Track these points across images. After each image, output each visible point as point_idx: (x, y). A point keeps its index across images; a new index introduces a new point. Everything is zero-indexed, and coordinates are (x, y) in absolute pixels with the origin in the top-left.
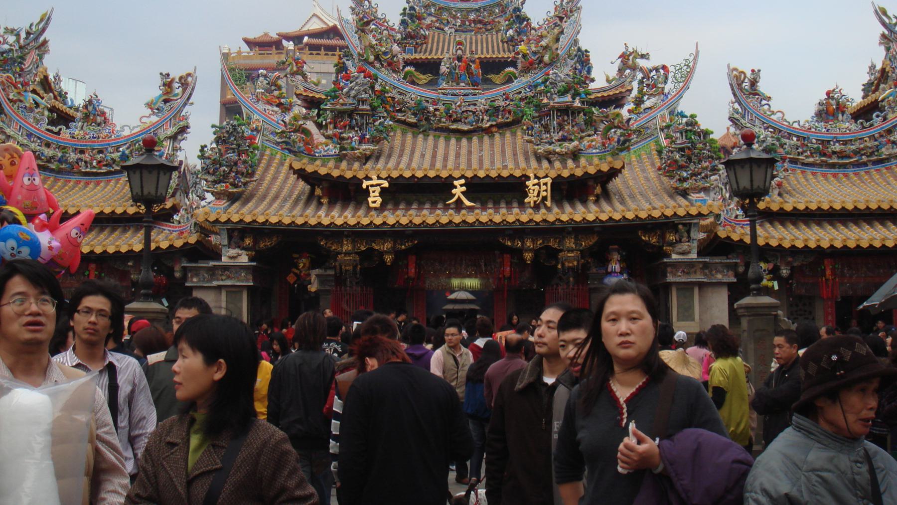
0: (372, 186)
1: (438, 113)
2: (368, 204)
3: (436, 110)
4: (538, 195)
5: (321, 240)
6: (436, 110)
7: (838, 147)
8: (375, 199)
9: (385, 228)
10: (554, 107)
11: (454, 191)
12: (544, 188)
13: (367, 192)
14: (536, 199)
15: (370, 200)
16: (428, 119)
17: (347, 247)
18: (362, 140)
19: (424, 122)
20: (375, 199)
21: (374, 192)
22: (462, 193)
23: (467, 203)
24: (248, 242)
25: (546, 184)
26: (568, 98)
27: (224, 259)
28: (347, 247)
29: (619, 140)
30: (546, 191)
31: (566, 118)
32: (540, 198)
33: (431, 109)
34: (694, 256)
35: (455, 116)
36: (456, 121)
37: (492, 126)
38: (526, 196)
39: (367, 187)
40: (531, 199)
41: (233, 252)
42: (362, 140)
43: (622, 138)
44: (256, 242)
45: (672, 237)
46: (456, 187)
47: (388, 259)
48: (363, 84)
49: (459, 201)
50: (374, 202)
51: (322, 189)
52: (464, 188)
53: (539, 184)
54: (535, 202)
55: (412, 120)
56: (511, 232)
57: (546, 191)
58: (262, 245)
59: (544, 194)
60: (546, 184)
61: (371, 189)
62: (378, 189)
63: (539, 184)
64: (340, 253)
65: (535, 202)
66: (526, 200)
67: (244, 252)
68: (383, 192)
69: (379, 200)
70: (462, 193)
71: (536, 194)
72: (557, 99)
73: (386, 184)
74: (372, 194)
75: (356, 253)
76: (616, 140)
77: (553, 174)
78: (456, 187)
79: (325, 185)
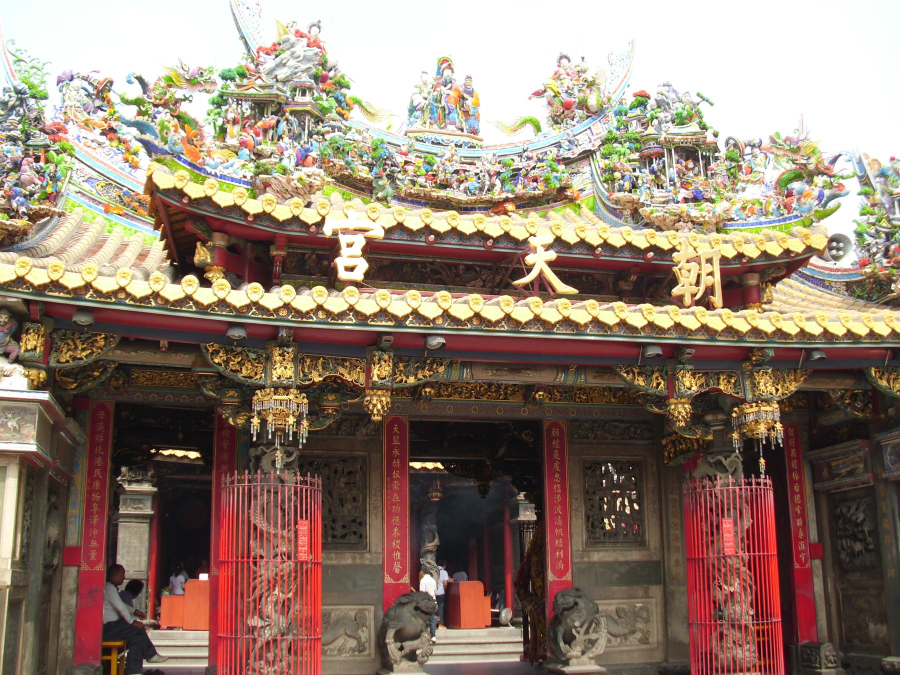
0: (346, 231)
1: (410, 168)
2: (334, 271)
3: (406, 163)
4: (698, 283)
5: (216, 353)
6: (406, 163)
8: (351, 262)
9: (382, 326)
10: (668, 141)
11: (529, 259)
12: (706, 268)
13: (332, 247)
14: (694, 289)
15: (341, 263)
16: (391, 177)
17: (283, 369)
18: (302, 160)
19: (384, 181)
20: (351, 262)
21: (350, 245)
22: (550, 264)
23: (561, 287)
24: (32, 342)
25: (709, 261)
26: (694, 127)
28: (283, 369)
29: (820, 197)
30: (711, 274)
31: (691, 164)
32: (702, 289)
33: (400, 159)
35: (441, 176)
36: (444, 186)
37: (507, 200)
38: (675, 282)
39: (335, 233)
40: (684, 288)
42: (302, 160)
43: (827, 192)
44: (50, 347)
46: (535, 250)
47: (378, 404)
48: (307, 59)
50: (351, 269)
51: (212, 249)
52: (552, 255)
53: (697, 260)
54: (693, 295)
55: (363, 173)
56: (659, 351)
57: (711, 274)
58: (65, 357)
59: (706, 281)
60: (709, 261)
61: (343, 240)
62: (360, 241)
63: (697, 260)
64: (262, 387)
65: (693, 295)
66: (676, 291)
67: (19, 368)
68: (371, 249)
69: (363, 266)
70: (550, 264)
72: (673, 129)
73: (378, 233)
74: (344, 251)
75: (301, 389)
76: (816, 193)
78: (535, 250)
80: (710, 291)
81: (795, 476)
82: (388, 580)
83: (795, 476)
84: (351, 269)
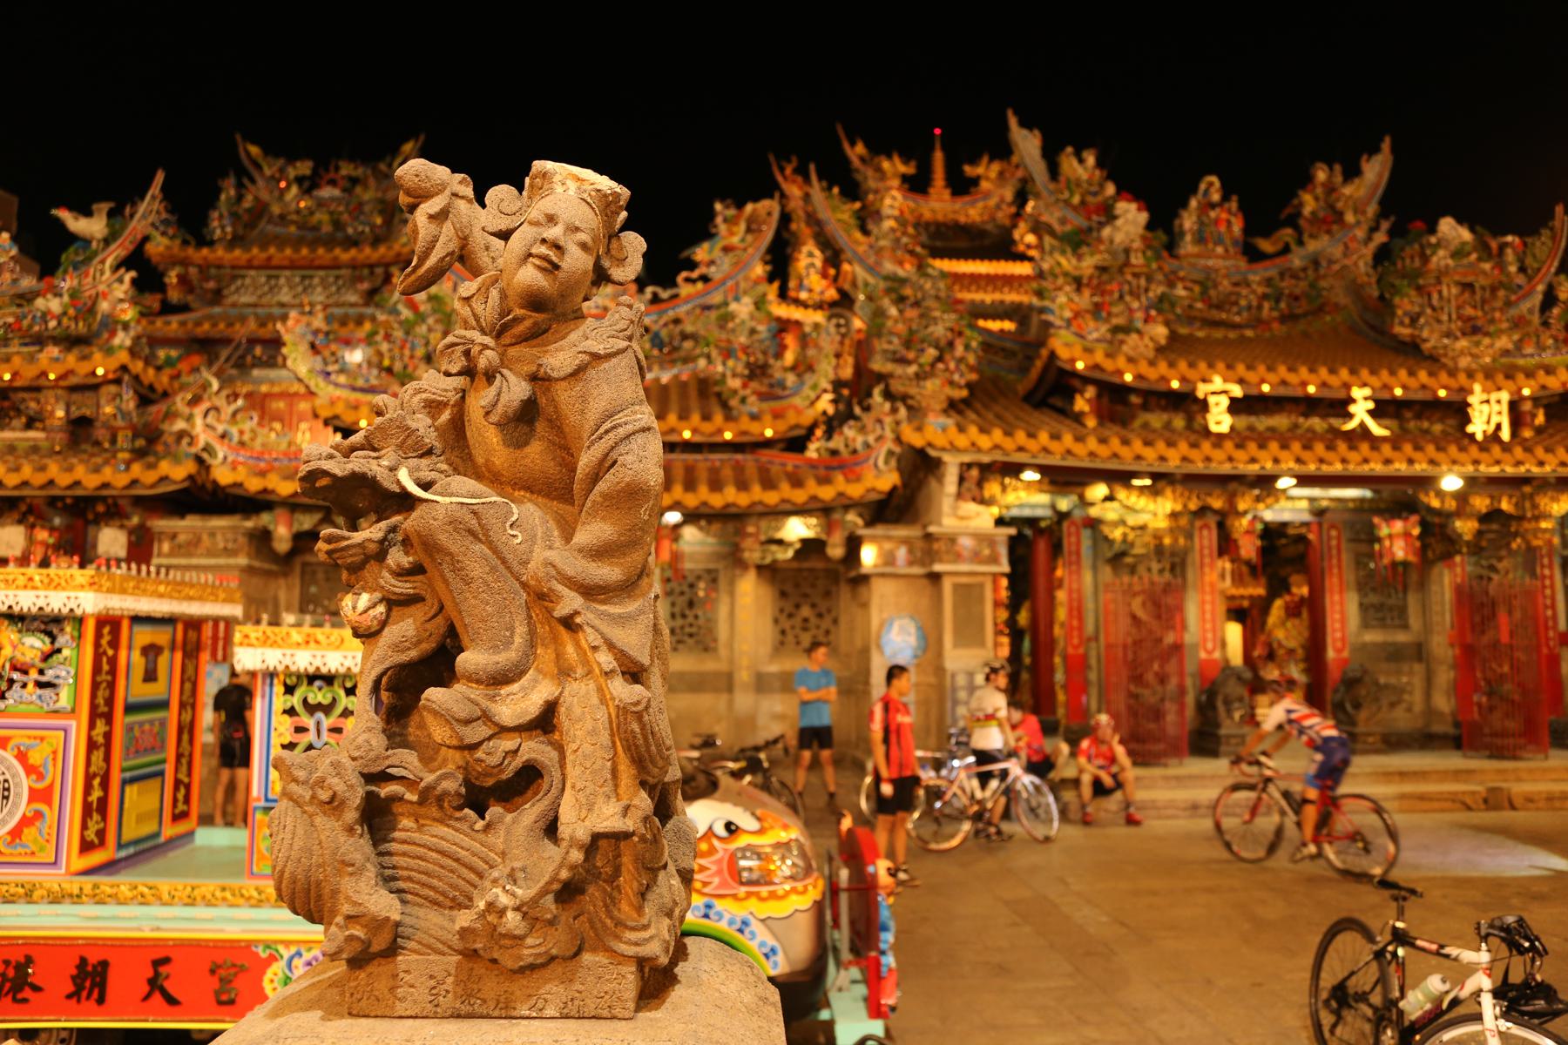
8: (1220, 420)
11: (1352, 409)
12: (1496, 408)
13: (1204, 406)
14: (1485, 427)
20: (1220, 420)
22: (1370, 412)
40: (1477, 428)
49: (1362, 425)
52: (1371, 405)
53: (1488, 401)
59: (1495, 420)
60: (1499, 402)
61: (1212, 400)
62: (1224, 402)
70: (1370, 412)
71: (1485, 418)
79: (1090, 392)
80: (1499, 427)
81: (1547, 572)
82: (1203, 655)
83: (1547, 572)
84: (1218, 423)
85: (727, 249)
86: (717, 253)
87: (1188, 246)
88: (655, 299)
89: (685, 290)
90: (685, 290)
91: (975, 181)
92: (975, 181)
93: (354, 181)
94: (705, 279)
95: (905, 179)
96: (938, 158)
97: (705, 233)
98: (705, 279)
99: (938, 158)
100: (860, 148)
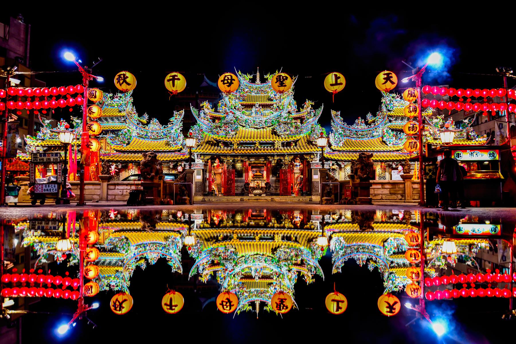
7: (361, 133)
24: (202, 157)
27: (196, 162)
34: (318, 161)
40: (276, 147)
41: (198, 160)
45: (312, 157)
77: (282, 140)
85: (176, 119)
86: (174, 120)
87: (254, 115)
88: (165, 127)
89: (169, 126)
90: (169, 126)
91: (267, 79)
92: (267, 79)
93: (121, 97)
94: (172, 124)
95: (250, 79)
96: (258, 74)
97: (172, 116)
98: (172, 124)
99: (258, 74)
100: (240, 72)
